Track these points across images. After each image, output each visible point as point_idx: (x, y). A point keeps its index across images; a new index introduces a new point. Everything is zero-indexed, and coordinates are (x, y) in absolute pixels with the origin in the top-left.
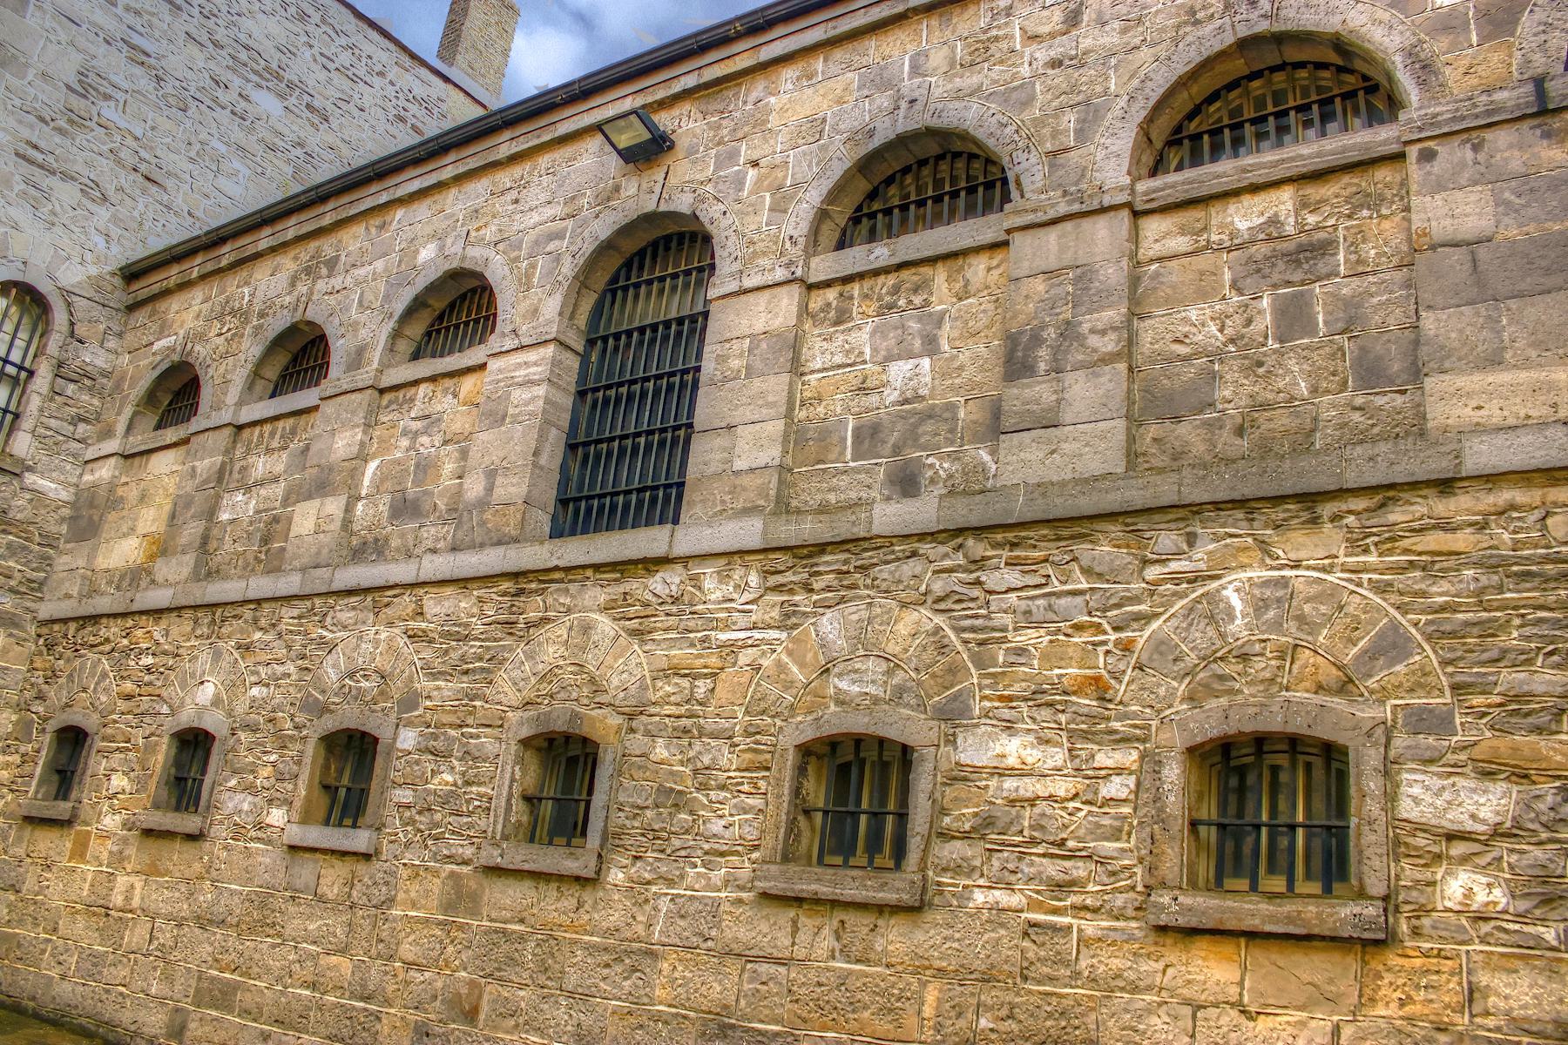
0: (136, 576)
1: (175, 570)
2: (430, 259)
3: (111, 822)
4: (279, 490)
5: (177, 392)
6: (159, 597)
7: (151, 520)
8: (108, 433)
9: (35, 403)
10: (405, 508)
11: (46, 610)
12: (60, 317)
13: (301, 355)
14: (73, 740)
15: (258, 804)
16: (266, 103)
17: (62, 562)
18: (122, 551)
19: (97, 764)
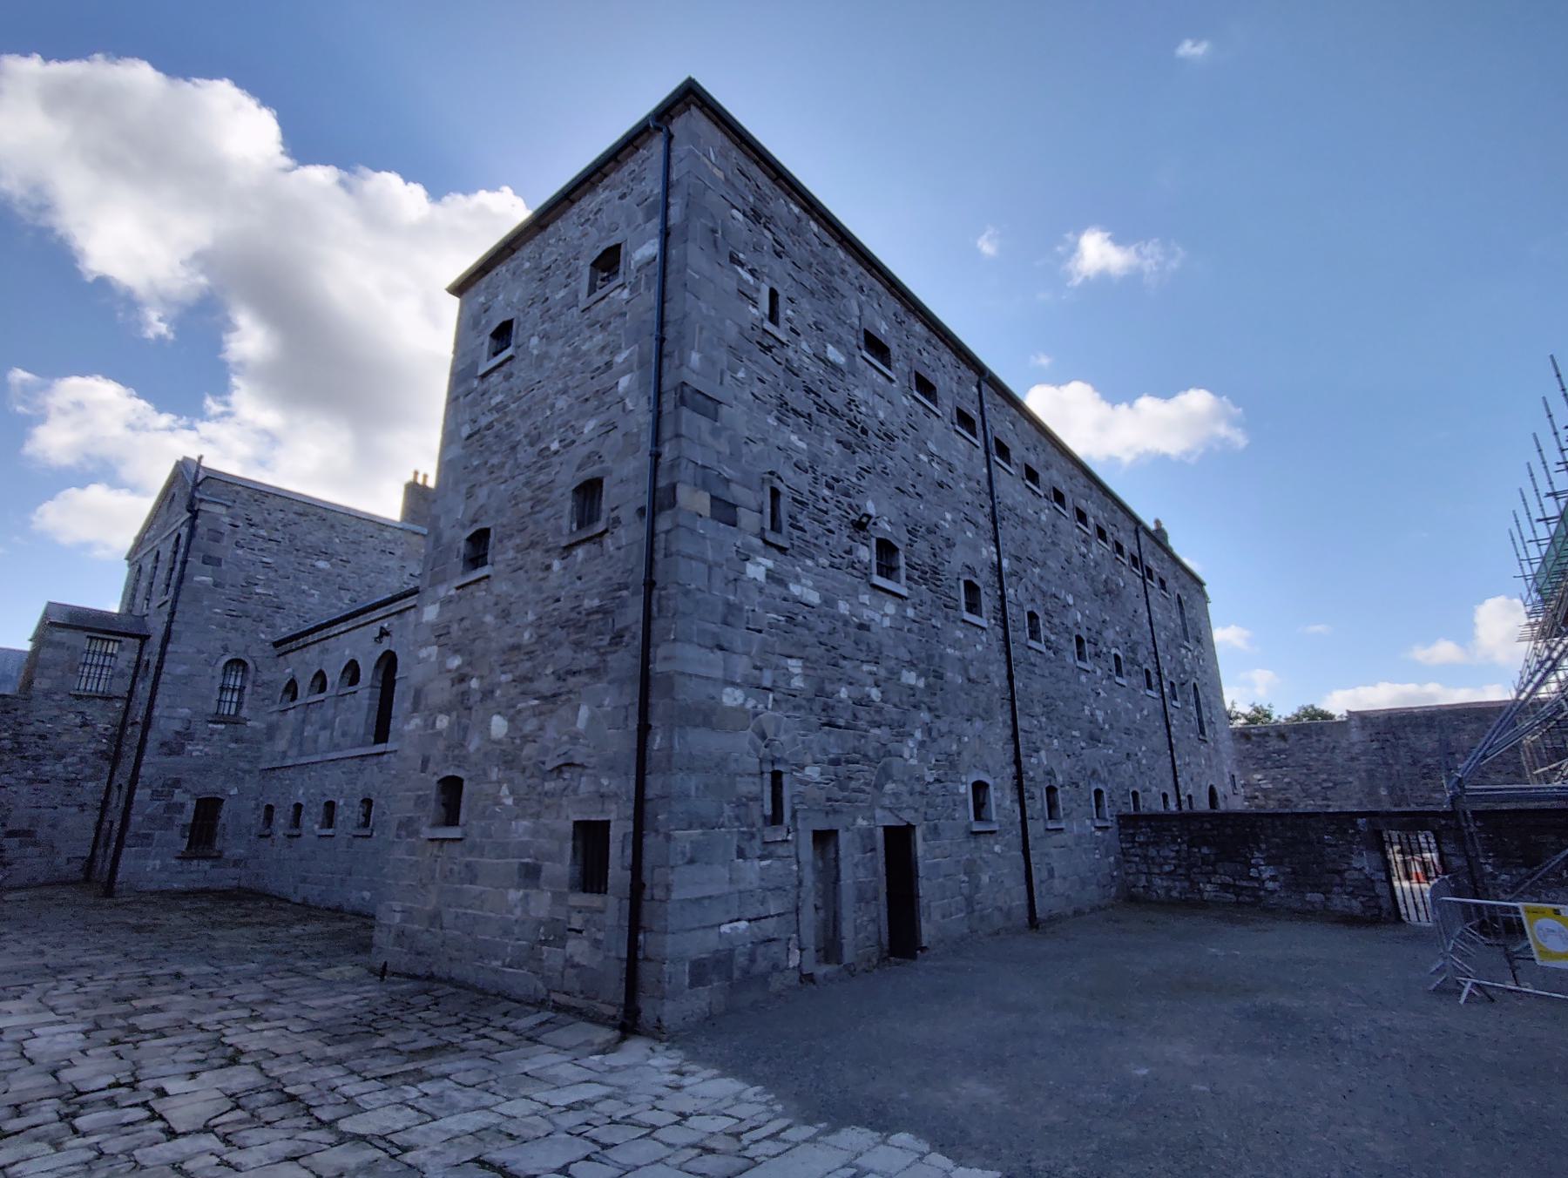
0: (284, 755)
1: (293, 752)
2: (348, 654)
3: (280, 833)
4: (317, 726)
5: (291, 688)
6: (289, 762)
7: (287, 734)
8: (274, 703)
9: (246, 698)
10: (344, 734)
11: (262, 766)
12: (251, 666)
13: (320, 681)
14: (270, 808)
15: (312, 823)
16: (322, 564)
17: (266, 749)
18: (281, 744)
19: (276, 816)
